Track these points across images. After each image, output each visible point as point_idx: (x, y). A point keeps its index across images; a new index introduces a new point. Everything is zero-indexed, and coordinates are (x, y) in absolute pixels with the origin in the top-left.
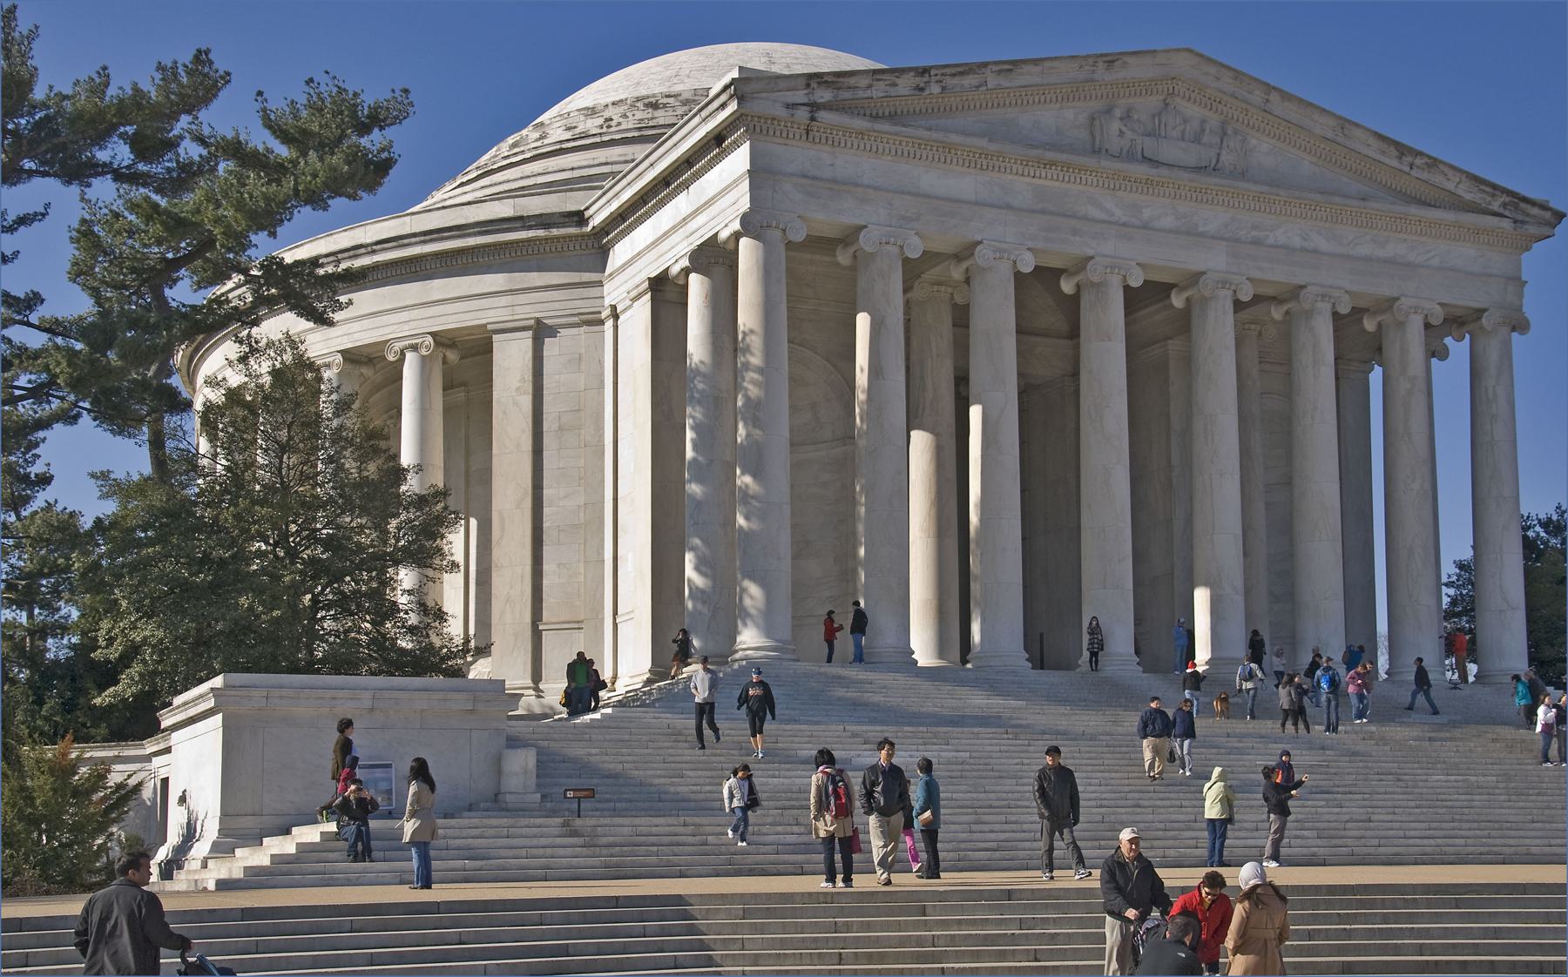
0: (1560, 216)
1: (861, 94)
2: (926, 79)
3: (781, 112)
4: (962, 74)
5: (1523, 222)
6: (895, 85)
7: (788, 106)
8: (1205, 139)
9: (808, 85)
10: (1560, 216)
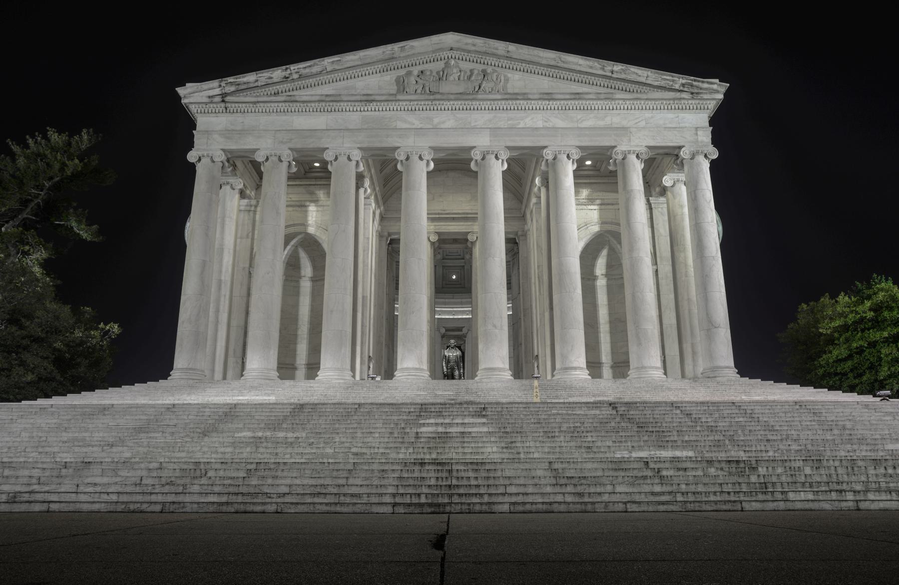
1: (252, 85)
3: (207, 100)
7: (209, 97)
8: (473, 78)
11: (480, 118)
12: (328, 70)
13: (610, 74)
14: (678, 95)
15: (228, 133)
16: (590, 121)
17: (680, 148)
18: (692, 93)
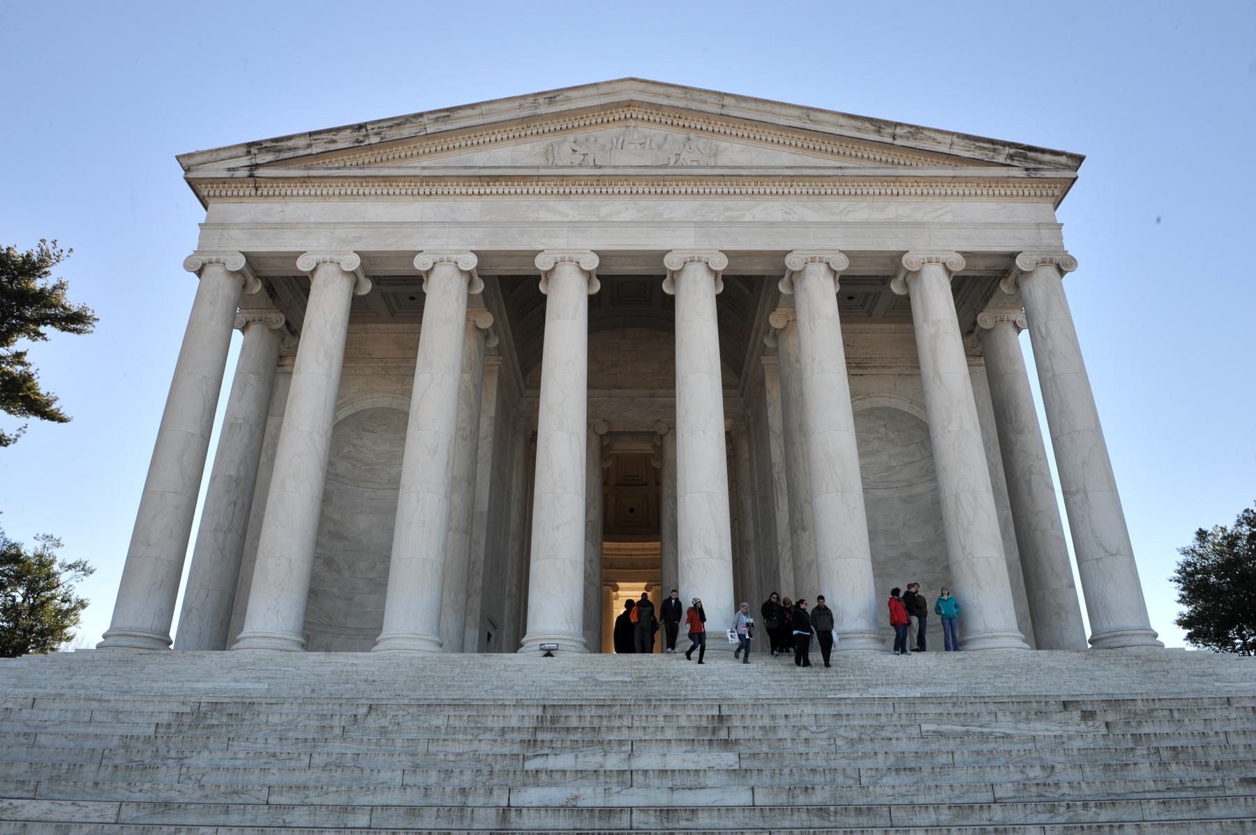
0: (1081, 159)
2: (363, 131)
4: (399, 125)
5: (1035, 169)
6: (334, 142)
7: (229, 170)
8: (666, 147)
9: (249, 153)
10: (1081, 159)
11: (678, 208)
12: (429, 131)
13: (890, 140)
14: (1003, 172)
15: (256, 227)
16: (860, 211)
17: (1013, 256)
18: (1027, 169)
